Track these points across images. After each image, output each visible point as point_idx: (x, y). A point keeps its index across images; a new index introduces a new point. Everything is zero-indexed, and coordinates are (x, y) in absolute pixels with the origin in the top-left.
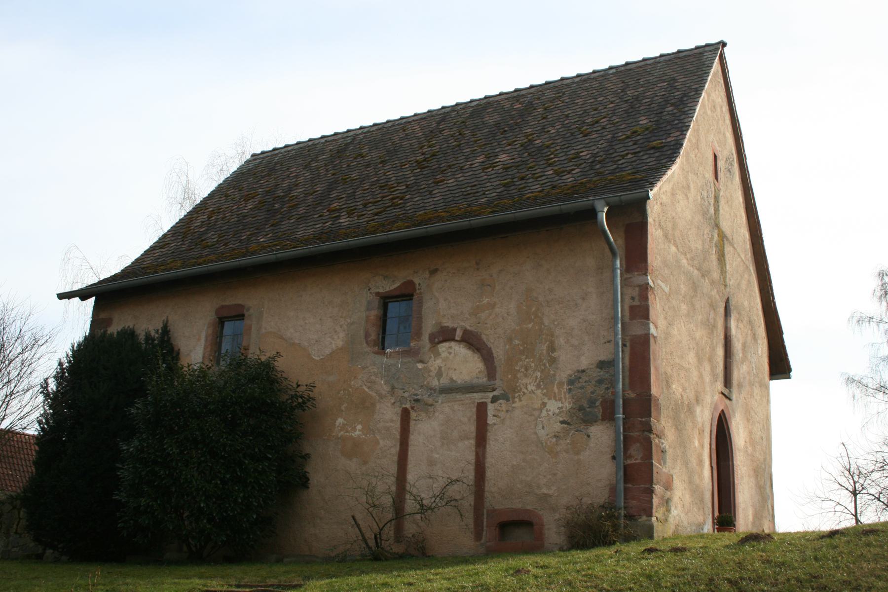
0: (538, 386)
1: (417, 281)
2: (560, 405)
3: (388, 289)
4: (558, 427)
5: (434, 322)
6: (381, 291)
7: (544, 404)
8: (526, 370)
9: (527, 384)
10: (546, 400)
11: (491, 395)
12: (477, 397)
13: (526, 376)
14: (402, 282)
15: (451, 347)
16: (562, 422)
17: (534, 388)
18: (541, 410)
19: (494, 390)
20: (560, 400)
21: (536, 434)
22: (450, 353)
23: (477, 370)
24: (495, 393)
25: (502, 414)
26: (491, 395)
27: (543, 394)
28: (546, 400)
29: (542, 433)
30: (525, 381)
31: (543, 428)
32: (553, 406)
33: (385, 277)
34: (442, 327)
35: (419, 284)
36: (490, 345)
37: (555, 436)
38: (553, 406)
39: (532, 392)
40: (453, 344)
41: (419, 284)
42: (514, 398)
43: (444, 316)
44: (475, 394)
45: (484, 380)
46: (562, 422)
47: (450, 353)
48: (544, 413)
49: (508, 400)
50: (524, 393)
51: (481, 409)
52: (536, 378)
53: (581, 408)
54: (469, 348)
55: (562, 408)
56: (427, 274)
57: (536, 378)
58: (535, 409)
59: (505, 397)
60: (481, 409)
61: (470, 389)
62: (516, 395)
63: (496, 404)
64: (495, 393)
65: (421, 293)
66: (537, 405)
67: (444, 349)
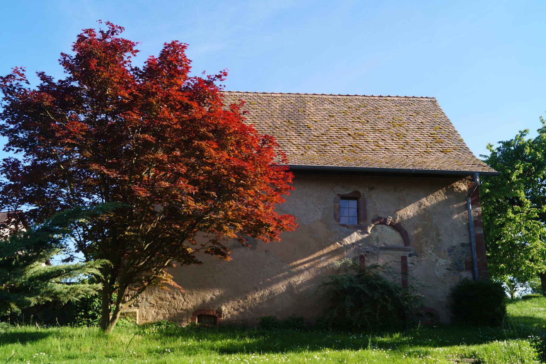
0: (433, 251)
1: (361, 191)
2: (446, 261)
3: (344, 193)
4: (446, 271)
5: (374, 214)
6: (341, 193)
7: (437, 260)
8: (426, 243)
9: (428, 250)
10: (438, 258)
11: (408, 253)
12: (401, 253)
13: (426, 246)
14: (352, 191)
15: (383, 227)
16: (447, 269)
17: (431, 252)
18: (436, 263)
19: (410, 251)
20: (445, 259)
21: (434, 273)
22: (383, 230)
23: (398, 241)
24: (410, 252)
25: (415, 263)
26: (408, 253)
27: (437, 256)
28: (438, 258)
29: (437, 273)
30: (426, 248)
31: (438, 271)
32: (442, 261)
33: (343, 187)
34: (378, 217)
35: (363, 194)
36: (405, 229)
37: (444, 275)
38: (442, 261)
39: (431, 254)
40: (384, 226)
41: (363, 194)
42: (421, 256)
43: (379, 212)
44: (400, 252)
45: (402, 245)
46: (447, 269)
47: (383, 230)
48: (437, 264)
49: (417, 256)
50: (426, 254)
51: (404, 258)
52: (432, 248)
53: (456, 264)
54: (393, 229)
55: (446, 262)
56: (367, 189)
57: (432, 248)
58: (432, 262)
59: (416, 254)
60: (404, 258)
61: (399, 249)
62: (422, 254)
63: (412, 258)
64: (410, 252)
65: (364, 198)
66: (434, 260)
67: (379, 228)
